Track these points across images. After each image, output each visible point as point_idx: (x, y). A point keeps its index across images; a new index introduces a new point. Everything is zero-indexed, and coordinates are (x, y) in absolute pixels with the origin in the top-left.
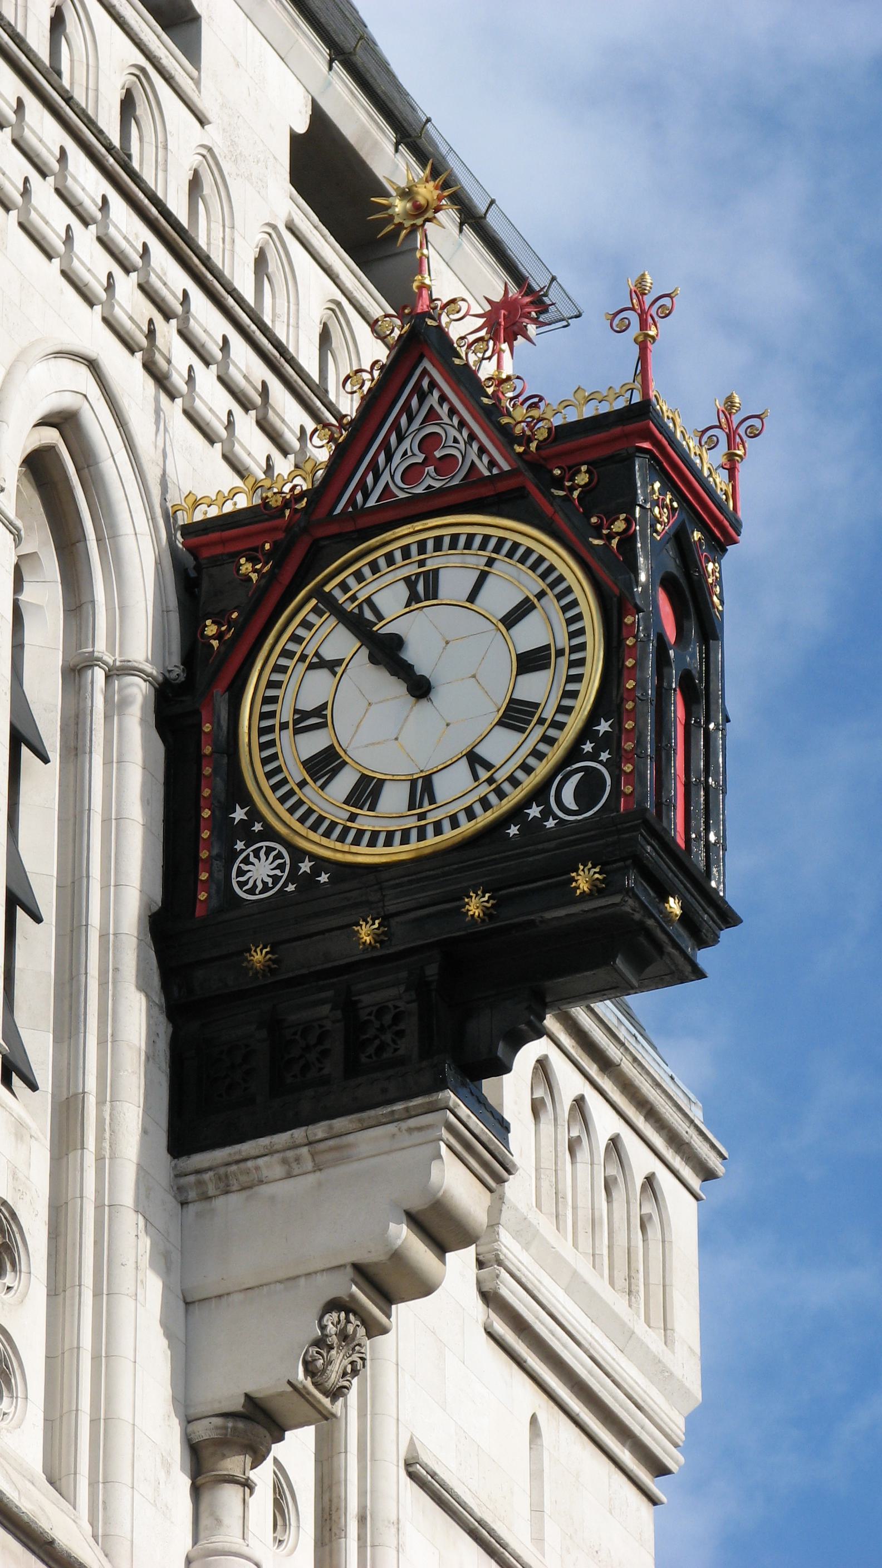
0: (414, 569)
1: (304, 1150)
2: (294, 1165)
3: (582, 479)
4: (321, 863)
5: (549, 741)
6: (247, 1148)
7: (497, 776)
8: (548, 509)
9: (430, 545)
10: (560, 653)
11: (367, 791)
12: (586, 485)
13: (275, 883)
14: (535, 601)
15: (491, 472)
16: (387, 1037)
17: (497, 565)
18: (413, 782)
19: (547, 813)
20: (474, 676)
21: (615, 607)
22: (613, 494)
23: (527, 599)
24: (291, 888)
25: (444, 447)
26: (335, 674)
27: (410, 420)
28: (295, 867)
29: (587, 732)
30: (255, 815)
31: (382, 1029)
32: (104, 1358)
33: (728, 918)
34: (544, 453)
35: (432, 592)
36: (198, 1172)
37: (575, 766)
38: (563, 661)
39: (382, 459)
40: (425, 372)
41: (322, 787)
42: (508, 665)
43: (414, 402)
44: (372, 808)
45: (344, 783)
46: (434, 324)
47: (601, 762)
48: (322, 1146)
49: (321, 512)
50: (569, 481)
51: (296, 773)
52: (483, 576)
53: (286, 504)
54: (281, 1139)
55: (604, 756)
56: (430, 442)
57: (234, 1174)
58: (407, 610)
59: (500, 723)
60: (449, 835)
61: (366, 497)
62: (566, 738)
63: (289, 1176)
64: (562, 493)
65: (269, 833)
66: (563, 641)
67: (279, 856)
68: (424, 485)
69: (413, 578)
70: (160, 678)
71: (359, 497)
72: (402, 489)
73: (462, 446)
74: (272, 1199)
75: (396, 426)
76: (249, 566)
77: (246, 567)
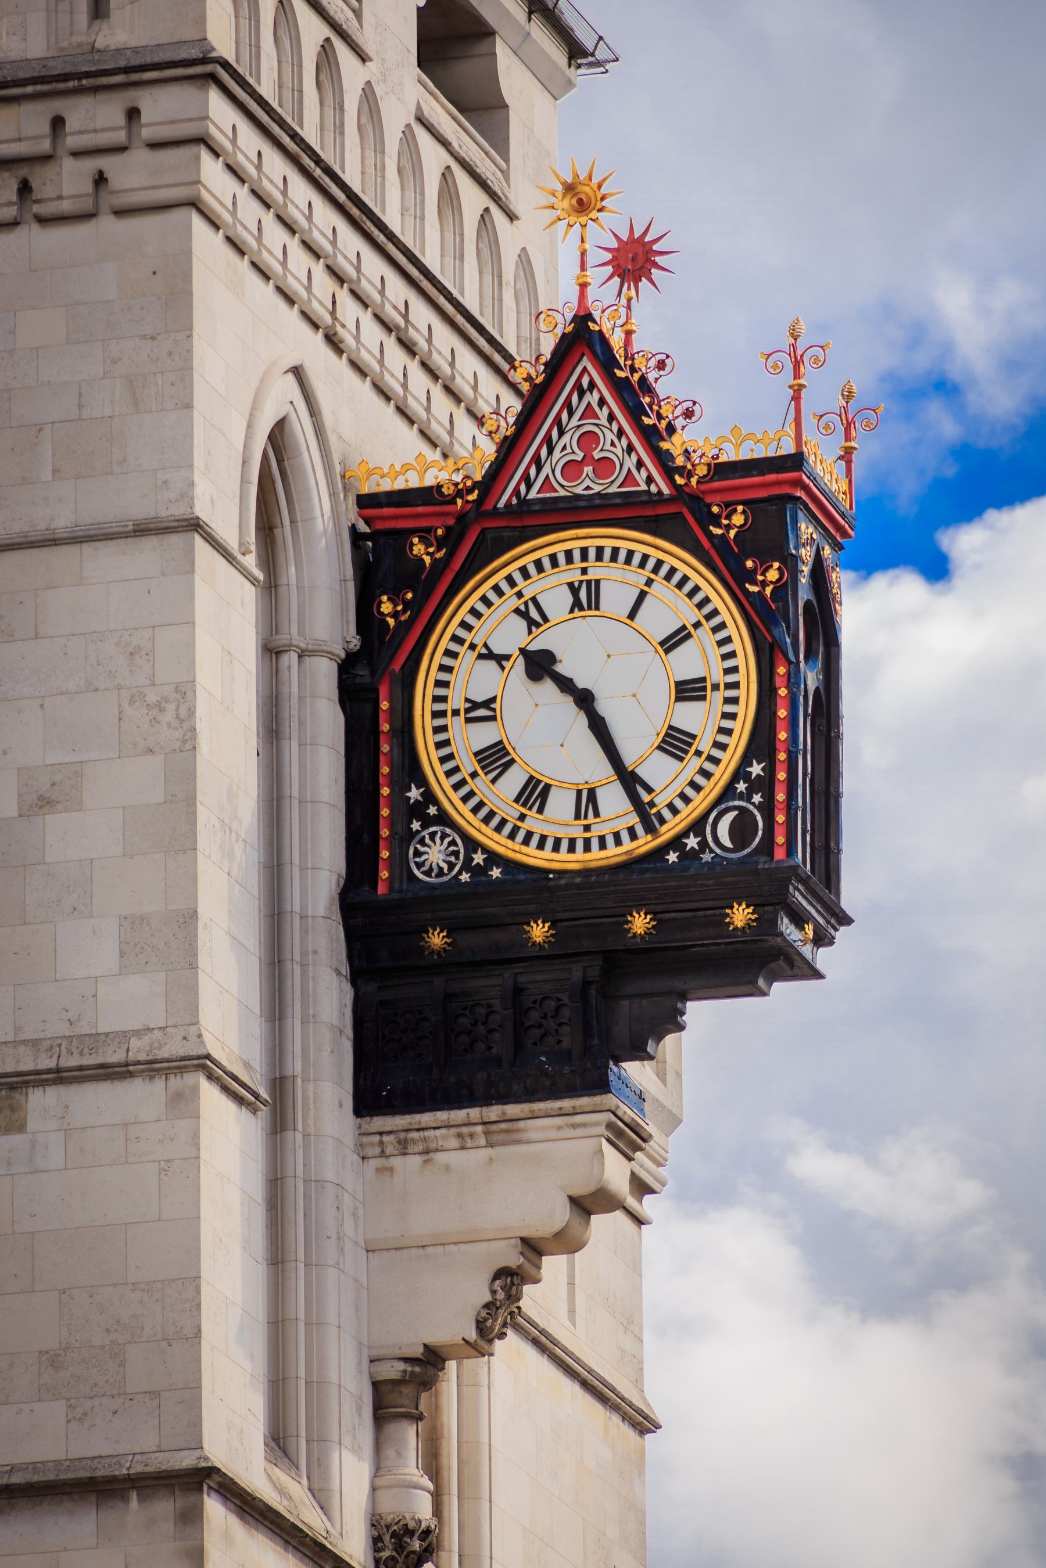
0: (576, 576)
1: (479, 1129)
2: (468, 1140)
3: (738, 520)
4: (493, 858)
5: (707, 775)
6: (426, 1118)
7: (657, 801)
8: (706, 543)
9: (592, 554)
10: (716, 687)
11: (535, 793)
12: (741, 526)
13: (450, 869)
14: (692, 630)
15: (649, 486)
16: (551, 1024)
17: (654, 585)
18: (579, 793)
19: (703, 845)
20: (634, 695)
21: (767, 654)
22: (768, 538)
23: (684, 628)
24: (465, 877)
25: (602, 450)
26: (503, 668)
27: (571, 414)
28: (468, 859)
29: (740, 773)
30: (429, 797)
31: (545, 1017)
32: (315, 1324)
33: (845, 920)
34: (702, 487)
35: (594, 603)
36: (381, 1134)
37: (731, 804)
38: (718, 697)
39: (544, 452)
40: (585, 369)
41: (494, 781)
42: (666, 692)
43: (575, 398)
44: (540, 811)
45: (513, 781)
46: (597, 328)
47: (753, 804)
48: (494, 1127)
49: (488, 506)
50: (726, 518)
51: (468, 764)
52: (643, 595)
53: (459, 493)
54: (459, 1115)
55: (757, 798)
56: (588, 440)
57: (413, 1140)
58: (571, 616)
59: (659, 748)
60: (613, 854)
61: (529, 487)
62: (722, 774)
63: (463, 1148)
64: (719, 532)
65: (443, 818)
66: (717, 676)
67: (453, 843)
68: (584, 485)
69: (576, 584)
70: (343, 655)
71: (523, 488)
72: (563, 486)
73: (619, 451)
74: (447, 1168)
75: (558, 421)
76: (422, 547)
77: (419, 549)
